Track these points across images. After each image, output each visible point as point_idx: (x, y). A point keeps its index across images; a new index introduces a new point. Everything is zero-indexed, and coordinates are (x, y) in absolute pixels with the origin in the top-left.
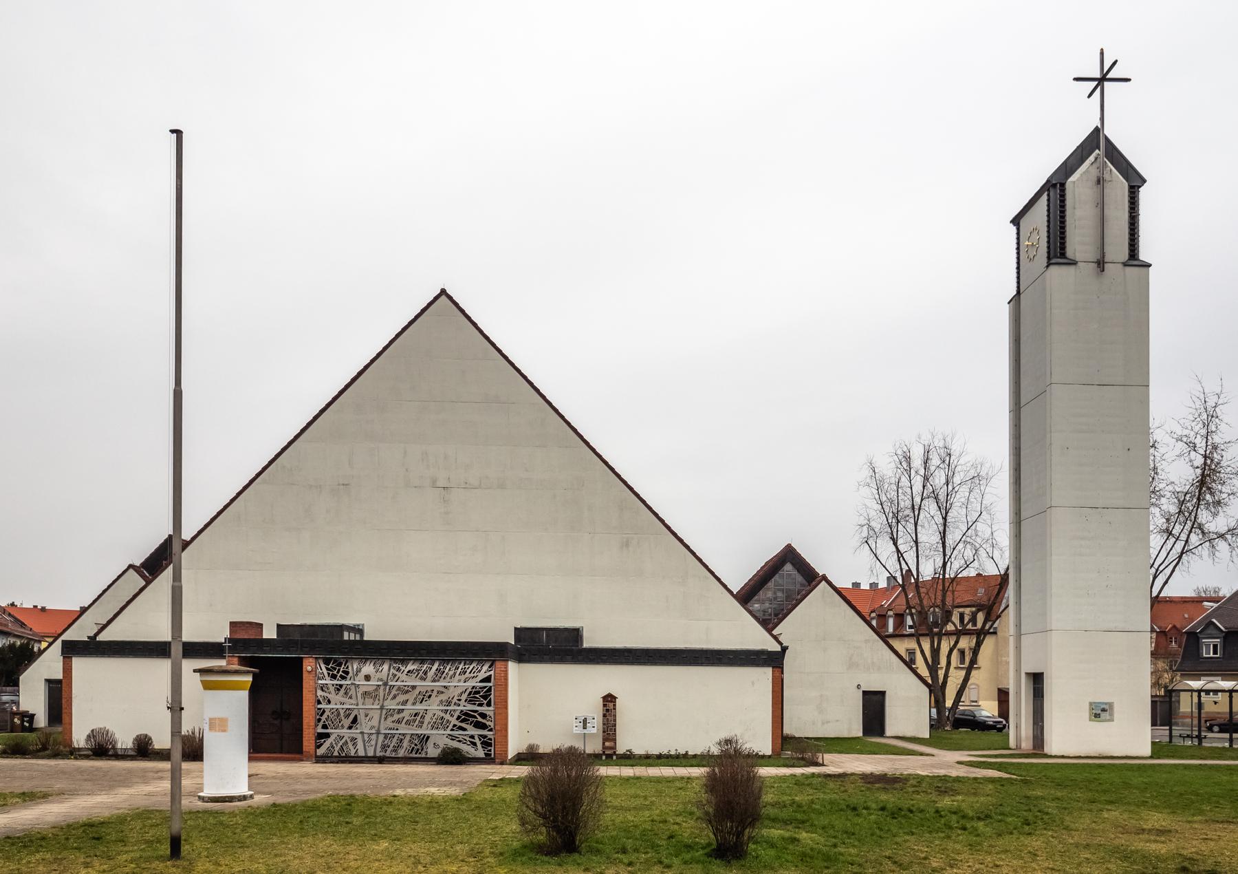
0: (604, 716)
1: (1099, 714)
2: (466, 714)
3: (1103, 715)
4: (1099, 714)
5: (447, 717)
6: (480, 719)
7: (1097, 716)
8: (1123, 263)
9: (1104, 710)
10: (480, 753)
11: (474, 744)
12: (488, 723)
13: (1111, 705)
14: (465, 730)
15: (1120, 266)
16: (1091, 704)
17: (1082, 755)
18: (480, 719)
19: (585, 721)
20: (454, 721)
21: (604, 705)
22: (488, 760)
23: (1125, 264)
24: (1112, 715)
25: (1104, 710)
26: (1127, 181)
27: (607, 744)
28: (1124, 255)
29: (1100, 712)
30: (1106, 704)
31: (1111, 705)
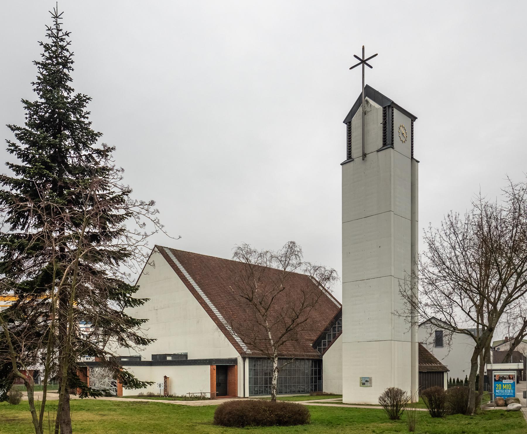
0: (165, 383)
1: (365, 383)
2: (112, 382)
3: (366, 383)
4: (365, 383)
5: (109, 383)
6: (115, 384)
7: (363, 384)
8: (377, 151)
9: (367, 381)
10: (115, 394)
11: (114, 391)
12: (116, 385)
13: (370, 379)
14: (112, 387)
15: (376, 152)
16: (361, 378)
17: (356, 403)
18: (115, 384)
19: (160, 384)
20: (110, 384)
21: (165, 380)
22: (116, 396)
23: (378, 151)
24: (371, 383)
25: (367, 381)
26: (382, 106)
27: (165, 392)
28: (380, 143)
29: (365, 382)
30: (368, 378)
31: (370, 379)
